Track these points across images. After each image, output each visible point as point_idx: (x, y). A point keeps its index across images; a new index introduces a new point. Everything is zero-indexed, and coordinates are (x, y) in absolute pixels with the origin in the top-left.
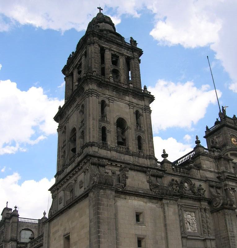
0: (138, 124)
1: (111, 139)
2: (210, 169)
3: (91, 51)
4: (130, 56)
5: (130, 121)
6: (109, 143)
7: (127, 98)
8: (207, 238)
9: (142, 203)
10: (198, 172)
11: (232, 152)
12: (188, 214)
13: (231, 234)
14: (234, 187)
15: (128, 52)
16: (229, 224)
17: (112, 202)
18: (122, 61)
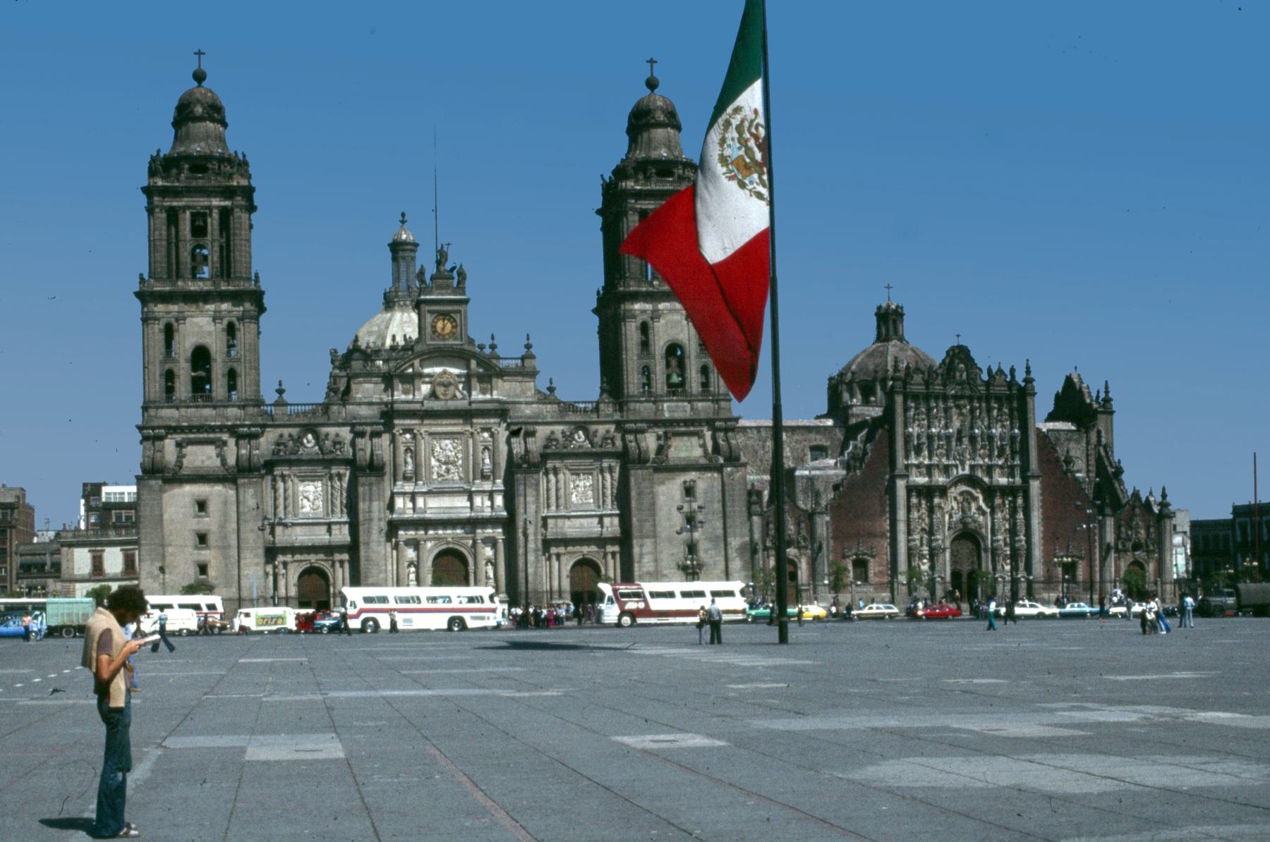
7: (211, 307)
18: (213, 222)
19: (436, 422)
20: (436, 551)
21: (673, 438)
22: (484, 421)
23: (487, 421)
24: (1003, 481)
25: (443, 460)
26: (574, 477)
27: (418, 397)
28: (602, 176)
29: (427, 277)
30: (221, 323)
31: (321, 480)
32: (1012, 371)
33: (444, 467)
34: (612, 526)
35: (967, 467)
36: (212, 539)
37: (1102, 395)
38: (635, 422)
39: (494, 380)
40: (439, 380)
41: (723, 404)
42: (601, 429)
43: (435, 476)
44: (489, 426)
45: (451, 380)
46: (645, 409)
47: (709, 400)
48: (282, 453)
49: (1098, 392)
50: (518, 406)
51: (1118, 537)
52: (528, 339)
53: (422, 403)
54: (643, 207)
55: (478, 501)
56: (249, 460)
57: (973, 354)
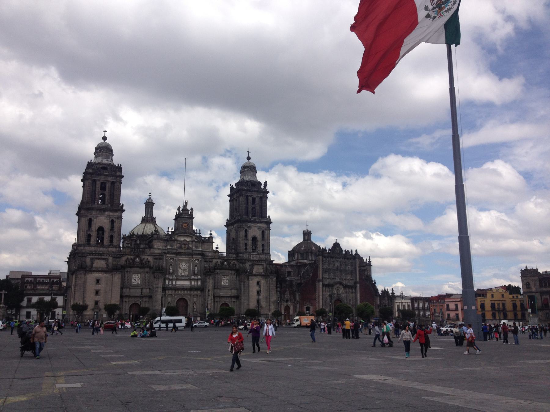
0: (112, 227)
1: (93, 240)
2: (159, 248)
3: (86, 185)
4: (113, 180)
5: (106, 226)
6: (91, 242)
7: (107, 213)
8: (144, 287)
9: (101, 274)
10: (149, 250)
11: (179, 235)
12: (136, 275)
13: (156, 286)
15: (114, 178)
16: (156, 281)
17: (83, 276)
19: (181, 256)
20: (178, 299)
22: (196, 257)
23: (197, 257)
24: (349, 284)
25: (182, 269)
26: (223, 277)
27: (176, 248)
28: (231, 185)
29: (181, 209)
30: (109, 220)
31: (140, 274)
32: (352, 251)
33: (182, 271)
35: (339, 279)
36: (102, 293)
37: (368, 260)
39: (200, 243)
41: (268, 256)
44: (198, 259)
45: (187, 243)
46: (246, 256)
47: (264, 255)
49: (366, 259)
50: (206, 252)
51: (380, 303)
52: (211, 232)
54: (247, 195)
55: (193, 283)
56: (117, 267)
57: (341, 246)
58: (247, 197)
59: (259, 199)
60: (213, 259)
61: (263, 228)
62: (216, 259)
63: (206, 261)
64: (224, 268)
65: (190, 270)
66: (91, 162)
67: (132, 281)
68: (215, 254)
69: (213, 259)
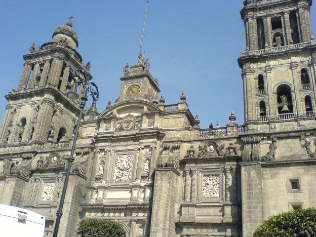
7: (33, 99)
14: (104, 148)
21: (278, 141)
26: (206, 177)
27: (112, 129)
33: (121, 172)
34: (228, 215)
38: (252, 135)
39: (157, 117)
40: (125, 120)
42: (227, 144)
43: (115, 178)
44: (149, 144)
45: (132, 119)
48: (39, 167)
53: (113, 133)
54: (259, 15)
58: (260, 21)
59: (287, 16)
60: (182, 142)
61: (304, 63)
62: (189, 141)
63: (166, 149)
64: (207, 157)
65: (134, 168)
66: (34, 45)
67: (41, 195)
68: (191, 132)
69: (182, 142)
